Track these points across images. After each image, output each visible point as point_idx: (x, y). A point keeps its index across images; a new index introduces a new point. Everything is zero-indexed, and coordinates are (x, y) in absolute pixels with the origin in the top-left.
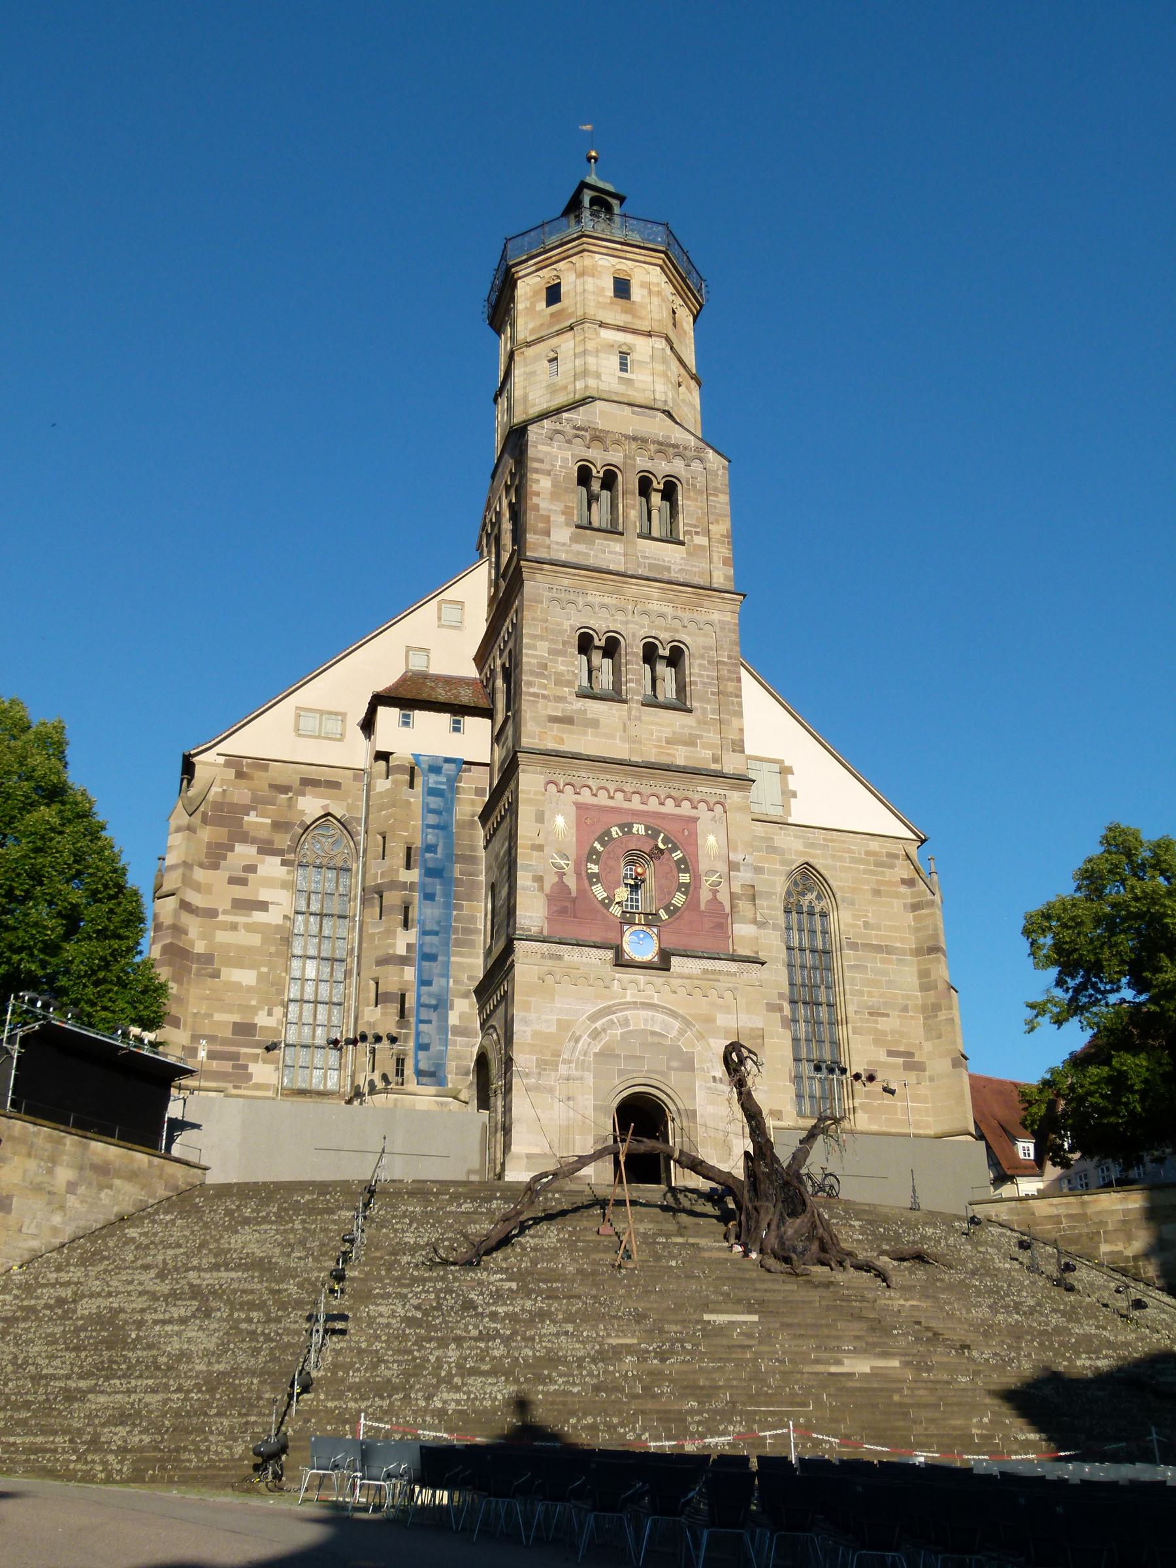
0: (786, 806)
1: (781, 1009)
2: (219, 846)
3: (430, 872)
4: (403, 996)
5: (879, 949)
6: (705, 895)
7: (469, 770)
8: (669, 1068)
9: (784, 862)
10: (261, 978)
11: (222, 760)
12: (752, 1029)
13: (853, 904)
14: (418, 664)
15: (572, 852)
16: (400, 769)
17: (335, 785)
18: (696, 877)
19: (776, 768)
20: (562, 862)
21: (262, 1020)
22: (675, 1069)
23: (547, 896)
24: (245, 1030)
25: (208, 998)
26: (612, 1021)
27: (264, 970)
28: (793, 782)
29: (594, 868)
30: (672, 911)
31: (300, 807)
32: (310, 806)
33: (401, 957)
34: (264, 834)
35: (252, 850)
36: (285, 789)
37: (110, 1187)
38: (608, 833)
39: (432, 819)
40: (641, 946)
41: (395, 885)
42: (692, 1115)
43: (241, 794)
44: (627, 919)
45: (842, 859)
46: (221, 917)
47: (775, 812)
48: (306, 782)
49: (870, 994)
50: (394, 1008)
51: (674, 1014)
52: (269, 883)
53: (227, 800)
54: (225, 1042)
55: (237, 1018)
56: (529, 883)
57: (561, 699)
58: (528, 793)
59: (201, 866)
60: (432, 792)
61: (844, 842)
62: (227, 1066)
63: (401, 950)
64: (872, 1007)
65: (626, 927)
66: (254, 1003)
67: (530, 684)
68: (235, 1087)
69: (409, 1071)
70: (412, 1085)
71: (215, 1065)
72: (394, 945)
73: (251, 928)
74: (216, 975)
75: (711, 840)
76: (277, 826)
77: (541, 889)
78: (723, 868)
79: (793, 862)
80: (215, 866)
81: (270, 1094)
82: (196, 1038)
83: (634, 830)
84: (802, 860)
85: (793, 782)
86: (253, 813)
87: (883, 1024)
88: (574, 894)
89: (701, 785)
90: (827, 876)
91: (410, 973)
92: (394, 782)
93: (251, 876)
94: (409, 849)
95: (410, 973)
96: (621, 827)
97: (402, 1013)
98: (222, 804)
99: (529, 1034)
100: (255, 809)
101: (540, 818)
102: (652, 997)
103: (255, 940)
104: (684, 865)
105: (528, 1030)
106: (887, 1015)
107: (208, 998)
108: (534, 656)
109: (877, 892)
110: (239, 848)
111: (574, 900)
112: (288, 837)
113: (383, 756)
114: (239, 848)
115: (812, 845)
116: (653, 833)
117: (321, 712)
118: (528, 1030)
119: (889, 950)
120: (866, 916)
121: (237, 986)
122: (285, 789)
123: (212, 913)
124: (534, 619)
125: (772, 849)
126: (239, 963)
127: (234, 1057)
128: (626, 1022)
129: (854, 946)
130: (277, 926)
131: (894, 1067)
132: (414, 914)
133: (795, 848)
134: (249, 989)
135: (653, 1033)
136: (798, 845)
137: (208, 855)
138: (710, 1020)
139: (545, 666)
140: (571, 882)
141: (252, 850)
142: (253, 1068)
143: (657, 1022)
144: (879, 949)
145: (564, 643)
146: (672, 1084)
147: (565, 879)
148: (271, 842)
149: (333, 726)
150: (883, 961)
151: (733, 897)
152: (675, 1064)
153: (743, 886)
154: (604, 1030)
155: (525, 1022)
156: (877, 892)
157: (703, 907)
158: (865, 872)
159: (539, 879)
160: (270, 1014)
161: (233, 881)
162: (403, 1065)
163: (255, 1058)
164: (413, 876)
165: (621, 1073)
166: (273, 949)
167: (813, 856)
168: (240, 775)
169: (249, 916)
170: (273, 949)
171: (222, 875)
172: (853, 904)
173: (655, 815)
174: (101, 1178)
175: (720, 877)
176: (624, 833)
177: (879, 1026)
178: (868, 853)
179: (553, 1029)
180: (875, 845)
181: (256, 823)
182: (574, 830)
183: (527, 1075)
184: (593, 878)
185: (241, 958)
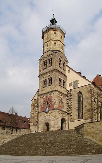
6: (52, 103)
42: (50, 124)
82: (34, 123)
116: (48, 99)
126: (36, 117)
129: (84, 99)
133: (78, 90)
136: (79, 90)
138: (52, 115)
151: (54, 103)
159: (40, 107)
180: (87, 86)
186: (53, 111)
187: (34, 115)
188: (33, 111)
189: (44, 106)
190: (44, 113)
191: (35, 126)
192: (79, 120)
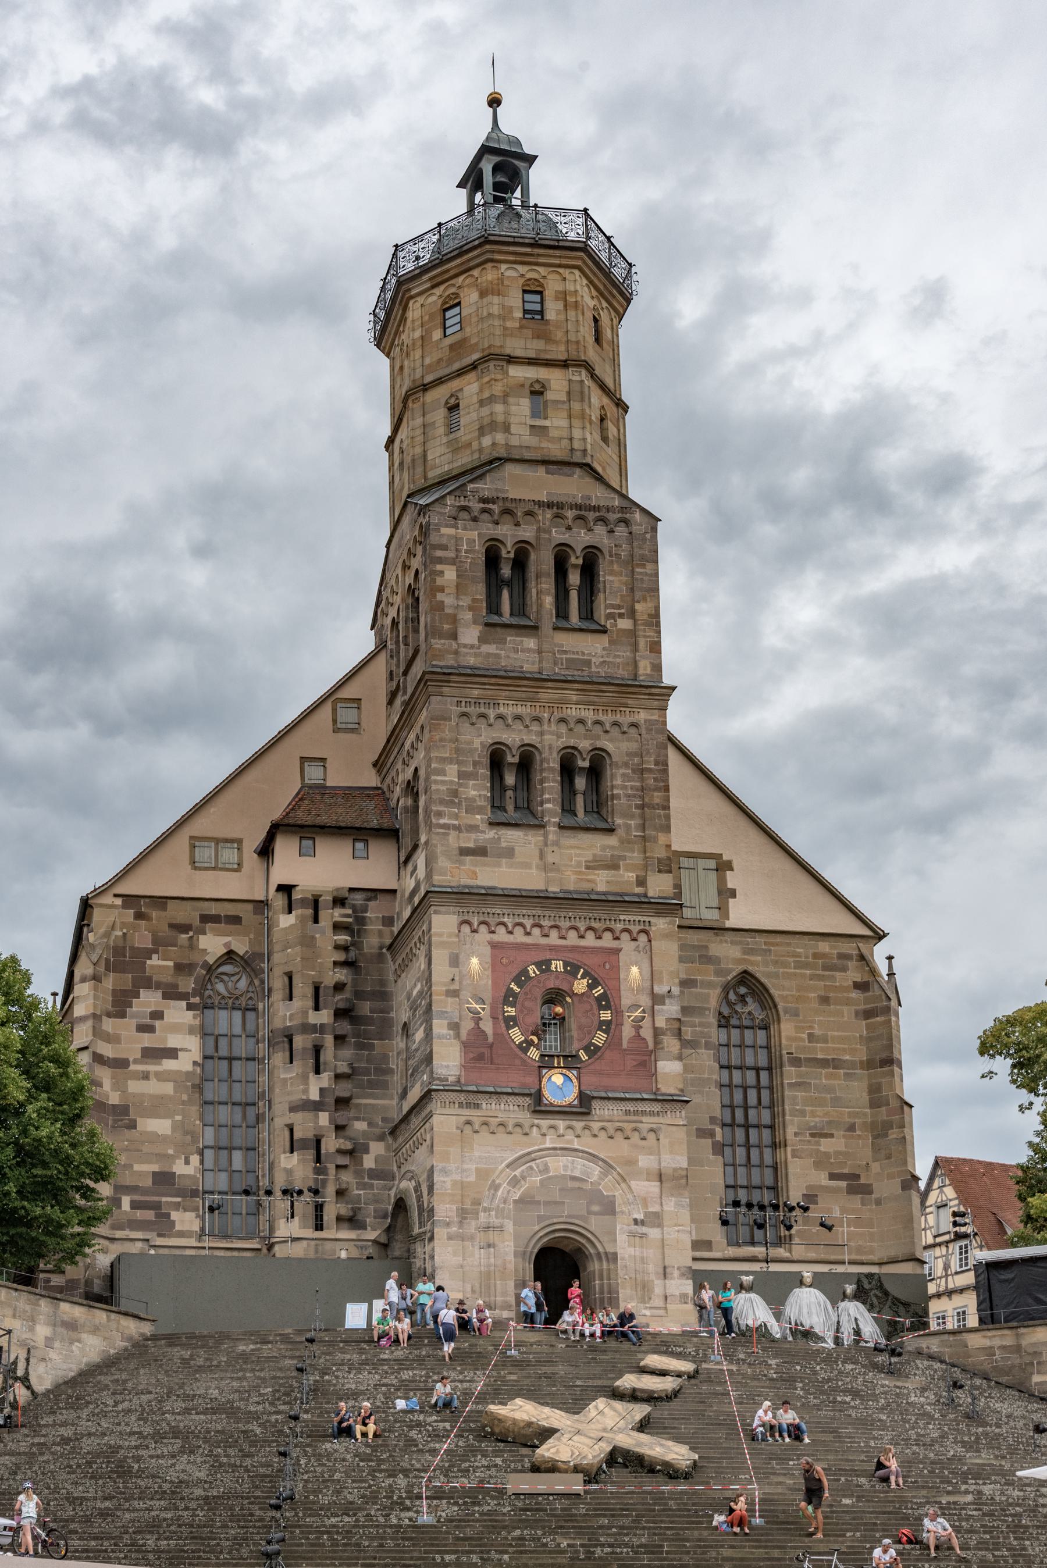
0: (723, 909)
2: (124, 993)
3: (340, 1014)
4: (318, 1142)
5: (824, 1063)
7: (376, 898)
8: (589, 1213)
9: (719, 973)
10: (174, 1128)
11: (119, 901)
12: (675, 1170)
13: (797, 1015)
14: (314, 774)
15: (488, 996)
16: (303, 902)
17: (236, 920)
18: (618, 1013)
21: (180, 1168)
22: (596, 1214)
23: (463, 1043)
24: (164, 1180)
26: (531, 1168)
27: (178, 1118)
29: (511, 1011)
30: (592, 1051)
31: (201, 947)
32: (212, 944)
33: (314, 1102)
34: (167, 978)
36: (184, 928)
37: (79, 1341)
38: (525, 972)
39: (341, 957)
40: (560, 1088)
41: (307, 1028)
42: (613, 1258)
44: (547, 1062)
45: (785, 965)
46: (133, 1067)
47: (711, 916)
48: (205, 919)
49: (813, 1114)
50: (310, 1155)
51: (593, 1157)
54: (145, 1191)
55: (156, 1168)
56: (445, 1031)
57: (473, 828)
58: (440, 935)
59: (109, 1015)
60: (337, 927)
62: (150, 1215)
63: (314, 1095)
65: (544, 1071)
66: (171, 1152)
67: (439, 814)
68: (160, 1235)
71: (139, 1214)
72: (306, 1091)
73: (161, 1077)
74: (132, 1126)
76: (180, 968)
77: (457, 1036)
78: (645, 1001)
79: (730, 971)
80: (122, 1015)
84: (741, 968)
86: (155, 956)
88: (490, 1039)
89: (624, 913)
90: (769, 985)
91: (324, 1119)
92: (297, 917)
93: (157, 1023)
94: (317, 989)
95: (324, 1118)
99: (449, 1185)
100: (156, 952)
102: (570, 1142)
103: (168, 1088)
105: (448, 1180)
108: (443, 782)
109: (825, 1000)
111: (491, 1046)
113: (286, 889)
115: (751, 951)
117: (217, 841)
119: (835, 1064)
120: (811, 1027)
121: (154, 1138)
122: (184, 928)
123: (121, 1064)
124: (442, 740)
125: (707, 959)
127: (156, 1206)
128: (546, 1169)
130: (188, 1073)
132: (328, 1054)
135: (573, 1178)
137: (115, 1003)
138: (631, 1162)
139: (455, 793)
141: (159, 994)
142: (175, 1215)
143: (578, 1166)
144: (824, 1063)
145: (475, 764)
146: (592, 1229)
148: (176, 986)
149: (229, 855)
150: (828, 1077)
151: (657, 1032)
152: (595, 1208)
154: (524, 1178)
155: (445, 1172)
156: (825, 1000)
157: (625, 1045)
158: (812, 977)
159: (455, 1027)
160: (187, 1162)
163: (177, 1206)
165: (540, 1219)
166: (185, 1097)
167: (752, 963)
169: (160, 1064)
170: (185, 1097)
172: (797, 1015)
173: (574, 949)
174: (70, 1333)
176: (542, 971)
178: (816, 956)
180: (824, 947)
181: (160, 966)
182: (489, 972)
183: (448, 1224)
184: (510, 1022)
185: (157, 1107)
186: (648, 1122)
187: (135, 1087)
188: (108, 1038)
189: (517, 1035)
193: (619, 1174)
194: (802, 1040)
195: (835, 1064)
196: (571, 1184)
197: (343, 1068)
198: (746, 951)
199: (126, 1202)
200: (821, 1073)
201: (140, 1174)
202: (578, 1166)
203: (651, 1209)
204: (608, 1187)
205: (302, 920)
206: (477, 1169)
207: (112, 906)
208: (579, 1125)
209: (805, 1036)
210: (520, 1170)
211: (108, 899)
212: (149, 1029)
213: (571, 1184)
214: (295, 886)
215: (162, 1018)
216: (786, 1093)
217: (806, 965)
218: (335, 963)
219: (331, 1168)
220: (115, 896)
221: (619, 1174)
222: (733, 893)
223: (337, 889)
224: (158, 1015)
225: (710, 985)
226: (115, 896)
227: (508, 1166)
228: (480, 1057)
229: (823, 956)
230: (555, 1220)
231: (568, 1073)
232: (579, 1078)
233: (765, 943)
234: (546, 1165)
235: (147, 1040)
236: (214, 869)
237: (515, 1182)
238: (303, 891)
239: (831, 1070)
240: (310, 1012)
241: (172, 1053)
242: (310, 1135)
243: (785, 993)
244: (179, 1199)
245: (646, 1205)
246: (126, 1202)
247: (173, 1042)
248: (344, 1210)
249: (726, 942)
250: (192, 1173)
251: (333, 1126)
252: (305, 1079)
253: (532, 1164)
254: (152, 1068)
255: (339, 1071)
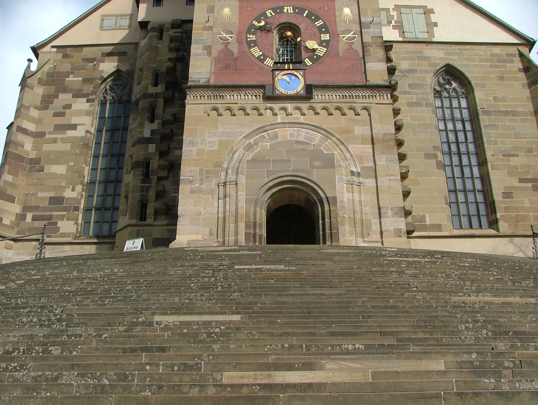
0: (430, 32)
1: (436, 157)
4: (147, 164)
5: (506, 113)
6: (342, 47)
8: (312, 167)
10: (69, 169)
12: (385, 135)
13: (484, 87)
15: (235, 30)
16: (153, 29)
18: (335, 35)
19: (422, 11)
20: (227, 36)
21: (68, 194)
22: (317, 167)
24: (57, 201)
25: (35, 184)
27: (72, 164)
28: (434, 18)
29: (252, 37)
31: (100, 68)
34: (76, 87)
35: (70, 96)
36: (91, 60)
39: (173, 55)
40: (290, 83)
41: (146, 96)
43: (66, 66)
44: (279, 66)
49: (502, 143)
50: (139, 171)
51: (316, 128)
52: (79, 113)
53: (56, 70)
54: (44, 209)
55: (52, 194)
56: (200, 51)
59: (36, 108)
61: (474, 50)
63: (147, 134)
64: (505, 151)
65: (277, 73)
66: (63, 184)
69: (150, 210)
70: (149, 221)
71: (37, 224)
72: (141, 132)
75: (347, 11)
77: (209, 54)
79: (437, 65)
80: (46, 108)
81: (70, 240)
82: (26, 208)
83: (285, 11)
84: (445, 62)
85: (434, 18)
86: (71, 76)
87: (514, 161)
88: (236, 55)
91: (152, 148)
93: (67, 111)
95: (152, 148)
96: (274, 10)
97: (146, 176)
98: (53, 73)
100: (73, 73)
101: (211, 10)
103: (67, 147)
104: (323, 29)
105: (195, 150)
106: (517, 156)
107: (35, 184)
110: (61, 96)
111: (236, 59)
112: (92, 86)
114: (61, 96)
115: (451, 54)
117: (117, 16)
118: (195, 150)
119: (514, 114)
127: (50, 218)
128: (276, 136)
129: (487, 113)
131: (526, 189)
132: (159, 111)
134: (61, 176)
135: (298, 142)
140: (234, 48)
141: (70, 96)
142: (60, 224)
143: (303, 134)
144: (506, 113)
146: (315, 179)
147: (229, 47)
148: (81, 90)
152: (317, 164)
153: (372, 37)
154: (256, 144)
155: (192, 143)
156: (502, 78)
157: (341, 55)
158: (491, 66)
159: (208, 49)
160: (73, 190)
161: (56, 115)
162: (146, 208)
163: (62, 218)
164: (160, 89)
165: (269, 173)
166: (78, 151)
168: (65, 56)
170: (78, 151)
171: (50, 112)
172: (484, 87)
175: (354, 34)
177: (511, 163)
178: (491, 55)
179: (216, 148)
180: (497, 50)
181: (73, 81)
183: (191, 182)
185: (58, 158)
187: (46, 147)
189: (256, 52)
190: (251, 99)
191: (32, 230)
192: (456, 232)
193: (338, 139)
194: (490, 101)
195: (514, 114)
196: (295, 147)
197: (168, 117)
198: (446, 54)
199: (29, 217)
200: (505, 119)
201: (42, 198)
202: (303, 134)
203: (365, 165)
204: (328, 147)
205: (151, 38)
206: (220, 141)
207: (50, 52)
208: (304, 106)
209: (491, 98)
210: (253, 139)
211: (47, 48)
212: (62, 115)
213: (295, 147)
214: (149, 22)
215: (70, 108)
216: (483, 131)
217: (487, 60)
218: (169, 59)
219: (154, 179)
220: (53, 47)
221: (338, 139)
222: (436, 24)
223: (173, 20)
224: (69, 107)
225: (425, 72)
226: (53, 47)
227: (245, 137)
228: (227, 67)
229: (497, 55)
230: (282, 174)
231: (295, 73)
232: (304, 76)
233: (459, 49)
234: (276, 133)
235: (60, 121)
236: (113, 29)
237: (249, 147)
238: (153, 24)
239: (511, 117)
240: (150, 86)
241: (74, 127)
242: (141, 159)
243: (475, 75)
244: (65, 213)
245: (361, 161)
246: (29, 217)
247: (74, 121)
248: (158, 205)
249: (434, 49)
250: (76, 196)
251: (158, 153)
252: (142, 125)
253: (265, 134)
254: (59, 136)
255: (165, 119)
